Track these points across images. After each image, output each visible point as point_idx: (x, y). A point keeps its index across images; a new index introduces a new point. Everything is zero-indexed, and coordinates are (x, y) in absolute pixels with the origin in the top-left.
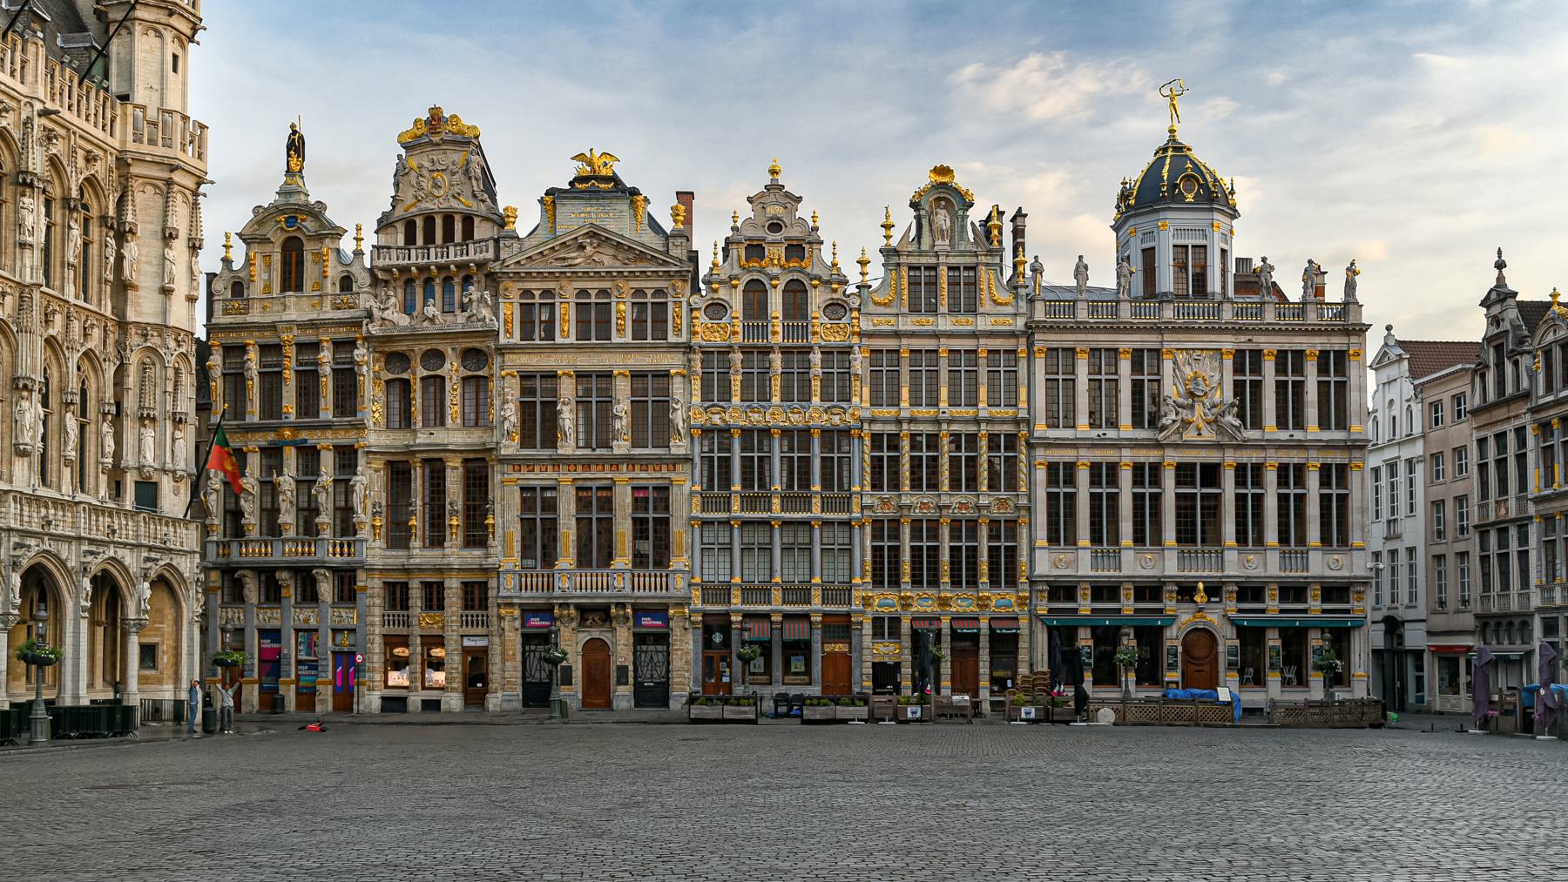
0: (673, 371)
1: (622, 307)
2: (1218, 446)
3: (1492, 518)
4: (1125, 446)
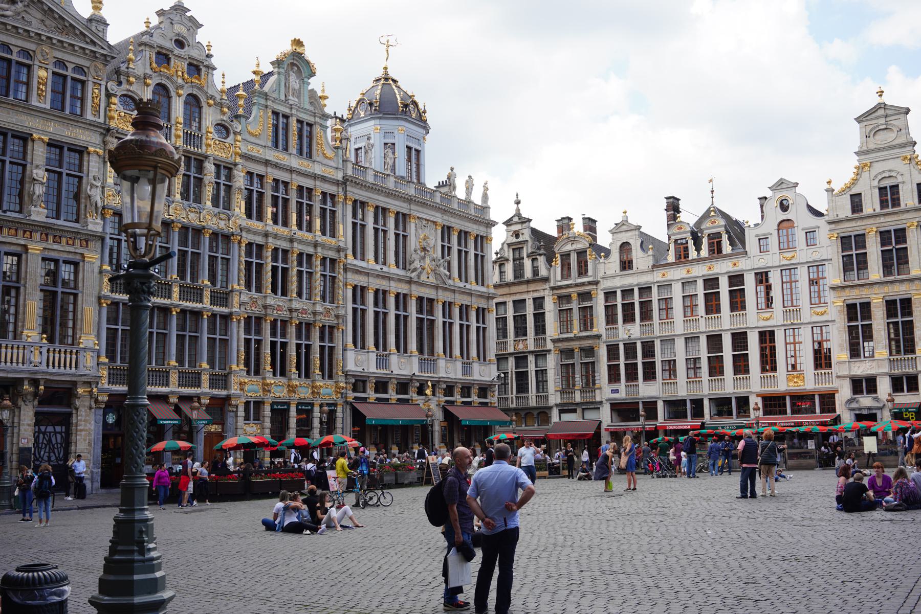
0: (90, 148)
1: (43, 73)
2: (437, 287)
3: (511, 350)
4: (394, 279)
